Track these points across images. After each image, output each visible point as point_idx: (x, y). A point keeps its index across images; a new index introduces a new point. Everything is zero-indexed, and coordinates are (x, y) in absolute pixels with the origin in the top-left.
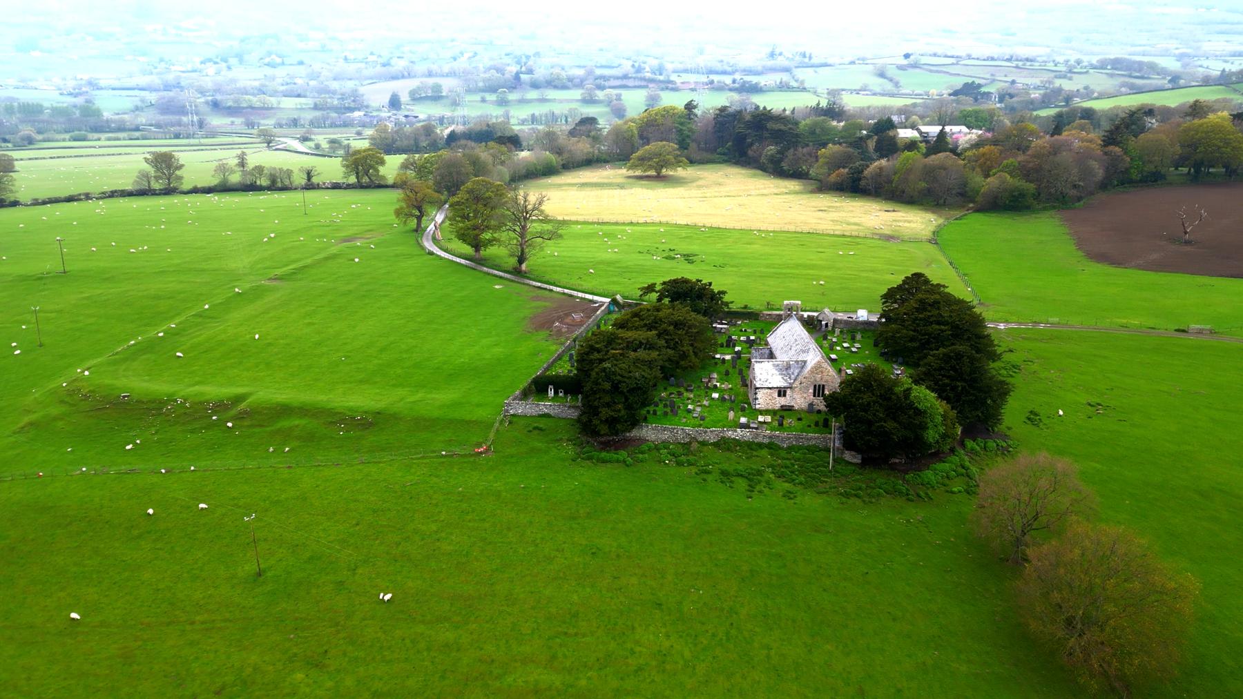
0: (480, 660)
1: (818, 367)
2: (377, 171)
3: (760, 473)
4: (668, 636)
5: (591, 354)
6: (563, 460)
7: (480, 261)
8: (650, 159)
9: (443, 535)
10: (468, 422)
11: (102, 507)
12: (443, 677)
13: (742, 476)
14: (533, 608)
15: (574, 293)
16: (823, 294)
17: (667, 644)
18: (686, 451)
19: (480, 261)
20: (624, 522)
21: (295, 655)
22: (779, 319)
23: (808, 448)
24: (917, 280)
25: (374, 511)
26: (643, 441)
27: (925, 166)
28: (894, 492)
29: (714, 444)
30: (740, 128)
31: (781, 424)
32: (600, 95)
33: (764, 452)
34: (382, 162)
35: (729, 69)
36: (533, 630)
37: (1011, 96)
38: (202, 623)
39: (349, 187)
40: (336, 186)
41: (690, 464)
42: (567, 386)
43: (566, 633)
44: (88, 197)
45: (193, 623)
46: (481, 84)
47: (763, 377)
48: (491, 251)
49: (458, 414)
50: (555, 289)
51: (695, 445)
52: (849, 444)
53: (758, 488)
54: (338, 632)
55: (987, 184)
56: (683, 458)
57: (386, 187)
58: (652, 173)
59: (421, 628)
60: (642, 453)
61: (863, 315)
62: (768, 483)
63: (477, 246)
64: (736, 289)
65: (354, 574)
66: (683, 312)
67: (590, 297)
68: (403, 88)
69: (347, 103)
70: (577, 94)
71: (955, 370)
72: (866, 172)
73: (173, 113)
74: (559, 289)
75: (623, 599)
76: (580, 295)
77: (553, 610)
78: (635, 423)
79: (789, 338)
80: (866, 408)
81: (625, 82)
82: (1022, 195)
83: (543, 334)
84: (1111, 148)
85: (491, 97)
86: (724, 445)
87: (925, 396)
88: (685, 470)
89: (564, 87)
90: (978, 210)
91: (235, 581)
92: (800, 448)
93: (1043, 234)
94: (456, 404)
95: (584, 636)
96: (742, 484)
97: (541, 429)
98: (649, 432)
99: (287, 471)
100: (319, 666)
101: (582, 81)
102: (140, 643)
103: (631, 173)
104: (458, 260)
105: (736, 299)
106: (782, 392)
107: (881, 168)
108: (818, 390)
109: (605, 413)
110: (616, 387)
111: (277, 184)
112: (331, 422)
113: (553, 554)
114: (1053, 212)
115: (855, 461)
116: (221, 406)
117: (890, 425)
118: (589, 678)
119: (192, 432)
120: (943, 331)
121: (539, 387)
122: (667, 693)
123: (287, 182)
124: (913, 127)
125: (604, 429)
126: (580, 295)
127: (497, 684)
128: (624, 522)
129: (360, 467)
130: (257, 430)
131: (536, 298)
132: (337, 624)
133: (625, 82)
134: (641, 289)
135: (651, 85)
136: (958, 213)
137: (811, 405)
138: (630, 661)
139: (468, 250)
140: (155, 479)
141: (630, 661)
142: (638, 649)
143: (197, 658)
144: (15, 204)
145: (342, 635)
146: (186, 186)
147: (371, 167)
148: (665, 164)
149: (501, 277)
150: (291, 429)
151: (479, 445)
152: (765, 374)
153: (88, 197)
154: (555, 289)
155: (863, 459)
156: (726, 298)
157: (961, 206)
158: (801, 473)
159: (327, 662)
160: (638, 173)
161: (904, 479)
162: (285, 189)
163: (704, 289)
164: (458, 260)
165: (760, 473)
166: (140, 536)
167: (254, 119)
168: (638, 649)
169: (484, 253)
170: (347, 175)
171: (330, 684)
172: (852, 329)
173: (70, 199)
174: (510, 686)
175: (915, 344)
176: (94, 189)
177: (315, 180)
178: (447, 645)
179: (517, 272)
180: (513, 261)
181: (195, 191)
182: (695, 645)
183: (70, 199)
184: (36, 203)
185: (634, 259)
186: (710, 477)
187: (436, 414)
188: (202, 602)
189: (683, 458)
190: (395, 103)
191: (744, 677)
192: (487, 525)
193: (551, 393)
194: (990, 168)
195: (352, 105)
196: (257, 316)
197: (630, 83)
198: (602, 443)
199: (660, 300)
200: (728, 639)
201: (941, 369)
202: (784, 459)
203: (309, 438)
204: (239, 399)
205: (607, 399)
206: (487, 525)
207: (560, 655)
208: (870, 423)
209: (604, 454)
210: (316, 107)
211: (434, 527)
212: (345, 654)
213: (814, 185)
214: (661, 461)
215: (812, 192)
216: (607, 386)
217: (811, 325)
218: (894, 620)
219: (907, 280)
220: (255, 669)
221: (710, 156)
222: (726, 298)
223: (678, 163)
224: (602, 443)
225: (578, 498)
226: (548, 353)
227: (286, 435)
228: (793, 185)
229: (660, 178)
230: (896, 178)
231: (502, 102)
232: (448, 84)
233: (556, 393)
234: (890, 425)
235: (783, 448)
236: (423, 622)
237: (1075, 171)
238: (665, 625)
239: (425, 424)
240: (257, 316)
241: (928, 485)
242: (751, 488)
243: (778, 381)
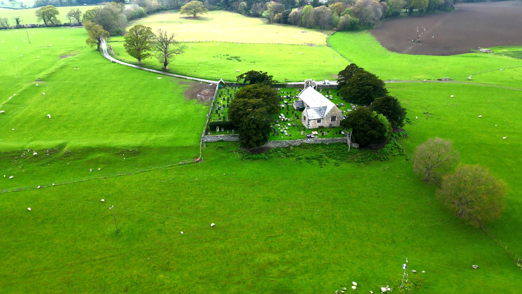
0: (240, 255)
1: (333, 110)
2: (55, 18)
3: (321, 157)
4: (312, 230)
6: (237, 160)
7: (141, 66)
8: (190, 9)
9: (198, 201)
10: (186, 147)
11: (14, 210)
12: (227, 265)
13: (315, 159)
14: (253, 228)
15: (199, 80)
16: (303, 73)
17: (314, 234)
19: (141, 66)
20: (275, 185)
21: (154, 267)
22: (300, 87)
23: (337, 144)
25: (160, 195)
26: (270, 148)
27: (315, 12)
28: (375, 158)
29: (299, 146)
31: (323, 135)
33: (320, 147)
34: (57, 13)
36: (257, 237)
38: (100, 260)
39: (41, 26)
40: (33, 26)
41: (292, 156)
42: (225, 126)
43: (271, 237)
45: (95, 260)
47: (311, 115)
48: (147, 60)
49: (178, 144)
50: (188, 78)
51: (292, 148)
52: (355, 140)
53: (323, 163)
54: (170, 253)
56: (288, 154)
57: (61, 26)
58: (192, 15)
59: (207, 245)
60: (271, 153)
62: (326, 160)
63: (139, 59)
64: (278, 75)
65: (164, 225)
66: (261, 88)
67: (207, 81)
71: (388, 106)
72: (290, 15)
74: (190, 78)
75: (289, 218)
76: (202, 80)
77: (262, 227)
80: (362, 126)
82: (355, 23)
83: (195, 101)
84: (383, 2)
86: (303, 146)
87: (382, 117)
88: (291, 159)
90: (338, 31)
91: (106, 237)
92: (334, 144)
94: (175, 139)
95: (279, 236)
96: (316, 162)
97: (222, 147)
98: (271, 144)
99: (105, 180)
100: (169, 270)
102: (72, 274)
103: (182, 16)
104: (129, 65)
106: (319, 121)
107: (296, 13)
108: (333, 118)
109: (255, 138)
110: (258, 127)
112: (117, 154)
113: (251, 203)
114: (366, 30)
115: (356, 147)
116: (53, 151)
117: (373, 132)
118: (289, 254)
119: (42, 165)
120: (370, 88)
121: (212, 128)
122: (323, 254)
123: (6, 25)
125: (255, 145)
126: (202, 80)
127: (252, 263)
128: (275, 185)
129: (142, 174)
130: (79, 161)
131: (181, 83)
132: (167, 249)
134: (237, 77)
136: (331, 32)
137: (331, 125)
138: (302, 244)
139: (135, 60)
140: (35, 192)
141: (302, 244)
142: (303, 238)
143: (106, 277)
145: (172, 254)
147: (51, 16)
148: (198, 11)
149: (157, 73)
150: (97, 159)
151: (197, 157)
152: (311, 114)
154: (188, 78)
155: (359, 146)
156: (273, 79)
157: (331, 29)
158: (338, 155)
159: (171, 267)
160: (186, 15)
161: (377, 152)
163: (265, 75)
164: (129, 65)
165: (321, 157)
166: (43, 222)
168: (303, 238)
169: (142, 61)
170: (39, 20)
171: (178, 277)
174: (258, 263)
175: (359, 95)
177: (21, 23)
178: (222, 250)
179: (165, 70)
180: (161, 65)
182: (325, 233)
186: (302, 161)
187: (168, 145)
188: (94, 250)
189: (288, 154)
191: (349, 243)
192: (216, 194)
193: (218, 130)
194: (341, 11)
196: (43, 101)
198: (251, 151)
199: (245, 82)
200: (336, 228)
201: (382, 105)
202: (329, 149)
203: (108, 163)
204: (61, 147)
205: (254, 132)
206: (216, 194)
207: (273, 246)
208: (365, 132)
209: (254, 156)
211: (192, 198)
212: (177, 262)
213: (267, 21)
214: (279, 156)
215: (267, 24)
216: (255, 126)
218: (394, 210)
219: (348, 67)
220: (138, 277)
221: (212, 6)
222: (273, 79)
223: (204, 10)
224: (251, 151)
225: (251, 177)
227: (96, 162)
229: (195, 18)
230: (303, 17)
233: (220, 129)
234: (373, 132)
235: (326, 145)
236: (207, 242)
237: (373, 13)
238: (310, 227)
240: (43, 101)
241: (386, 154)
242: (321, 164)
243: (318, 117)
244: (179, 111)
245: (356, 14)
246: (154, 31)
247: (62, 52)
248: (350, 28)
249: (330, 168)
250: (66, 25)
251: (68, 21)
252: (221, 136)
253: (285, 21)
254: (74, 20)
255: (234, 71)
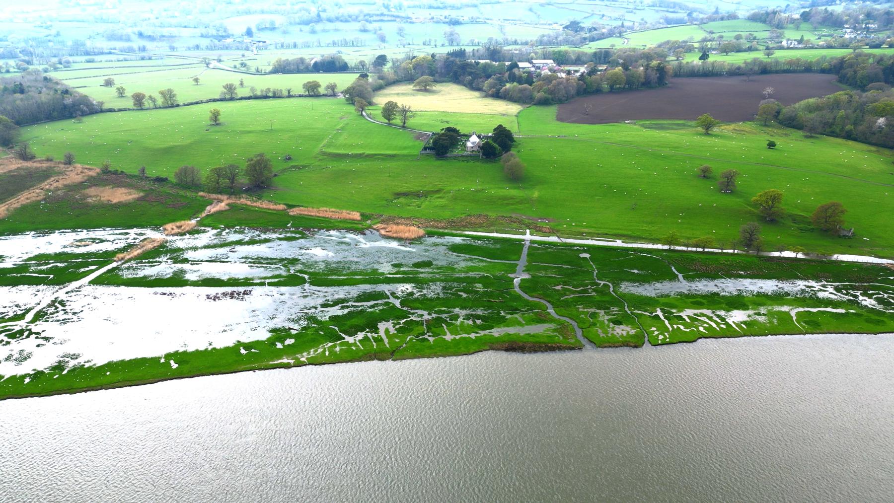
5: (435, 142)
7: (390, 124)
18: (456, 158)
19: (390, 124)
24: (500, 126)
30: (455, 68)
32: (370, 26)
35: (441, 6)
37: (595, 29)
39: (306, 96)
40: (300, 96)
42: (430, 148)
44: (202, 102)
46: (297, 20)
48: (393, 121)
55: (538, 95)
61: (490, 134)
64: (463, 130)
68: (252, 21)
69: (221, 33)
70: (357, 25)
73: (115, 40)
78: (446, 153)
79: (474, 139)
81: (382, 18)
85: (306, 28)
86: (462, 156)
87: (495, 145)
89: (347, 21)
93: (551, 112)
98: (448, 155)
101: (357, 17)
105: (462, 132)
111: (276, 96)
116: (360, 155)
121: (425, 149)
124: (530, 61)
133: (382, 18)
135: (398, 20)
144: (178, 105)
146: (240, 96)
152: (469, 144)
153: (202, 102)
162: (280, 97)
167: (175, 45)
172: (487, 137)
173: (197, 103)
176: (204, 99)
179: (404, 127)
181: (242, 99)
183: (197, 103)
184: (184, 105)
185: (432, 122)
190: (249, 33)
195: (224, 34)
197: (386, 18)
203: (382, 159)
210: (202, 36)
217: (479, 137)
221: (442, 79)
226: (421, 144)
227: (378, 159)
228: (477, 94)
229: (426, 90)
231: (313, 32)
232: (279, 20)
239: (404, 156)
244: (411, 144)
245: (551, 92)
246: (399, 105)
247: (339, 116)
248: (544, 103)
249: (471, 164)
250: (324, 95)
251: (324, 92)
252: (428, 151)
253: (497, 96)
254: (330, 92)
255: (439, 128)
